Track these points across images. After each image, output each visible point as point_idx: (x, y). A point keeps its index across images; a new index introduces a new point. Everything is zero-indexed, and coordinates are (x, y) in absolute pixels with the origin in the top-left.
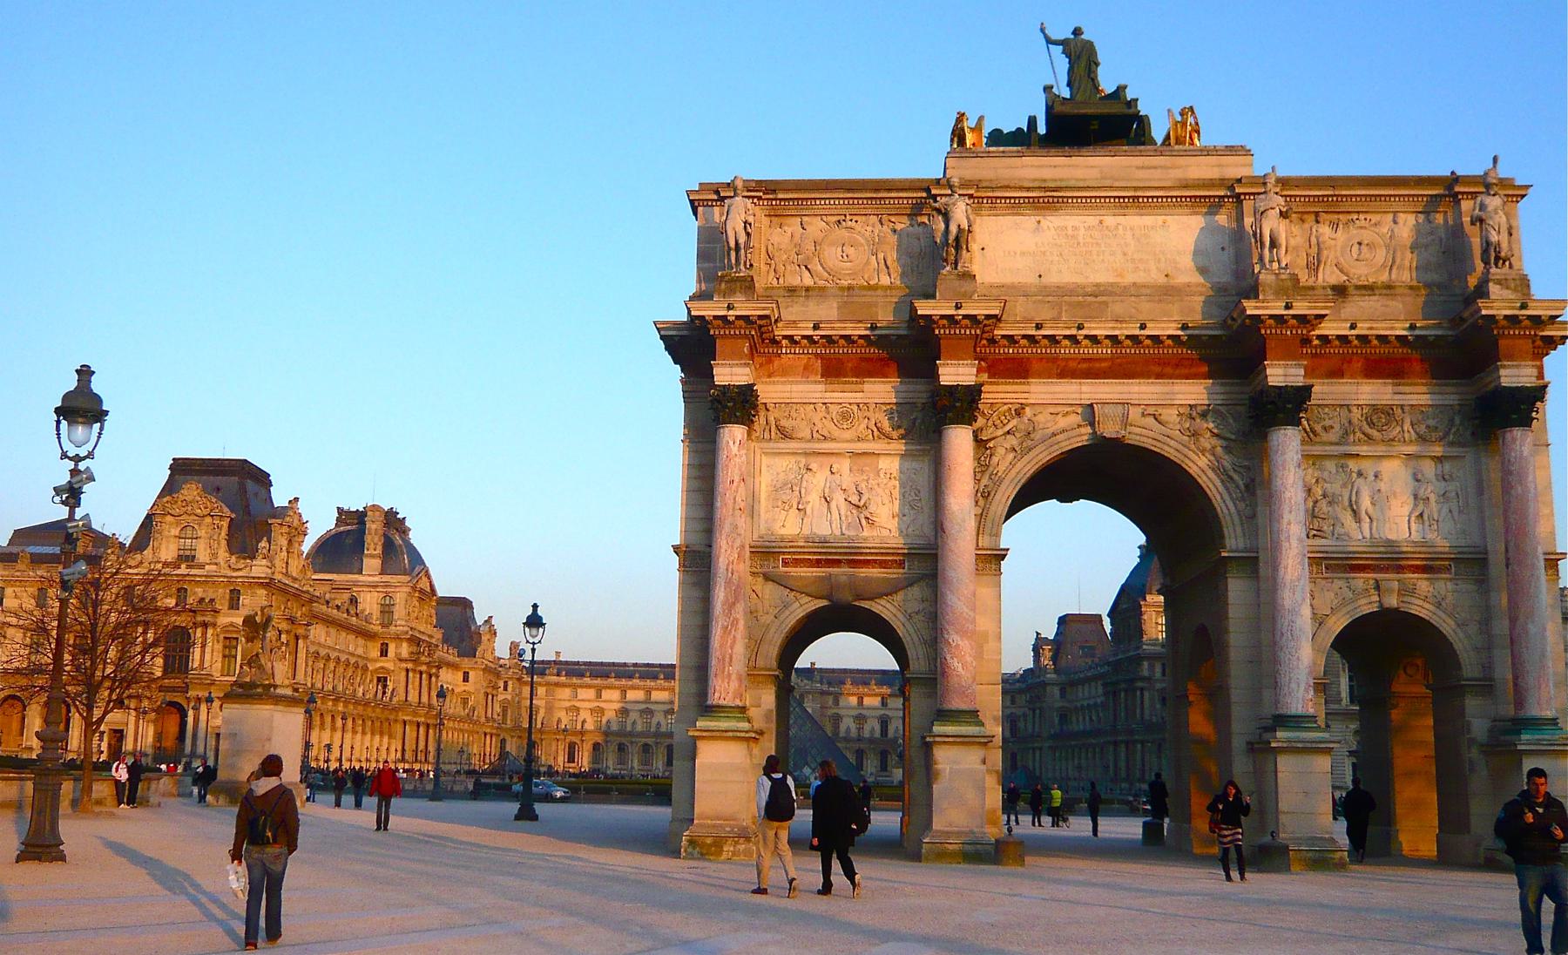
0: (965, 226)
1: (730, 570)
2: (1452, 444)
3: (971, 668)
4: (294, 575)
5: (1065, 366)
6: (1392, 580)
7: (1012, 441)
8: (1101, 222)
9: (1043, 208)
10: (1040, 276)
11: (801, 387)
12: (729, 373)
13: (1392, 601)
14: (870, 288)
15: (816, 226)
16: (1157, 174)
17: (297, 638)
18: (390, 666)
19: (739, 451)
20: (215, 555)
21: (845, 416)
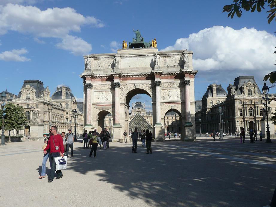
0: (118, 61)
2: (181, 87)
4: (49, 101)
6: (173, 105)
7: (125, 89)
11: (98, 83)
12: (88, 82)
13: (173, 108)
14: (108, 69)
15: (100, 61)
16: (145, 52)
17: (50, 112)
18: (68, 116)
20: (33, 98)
21: (104, 86)
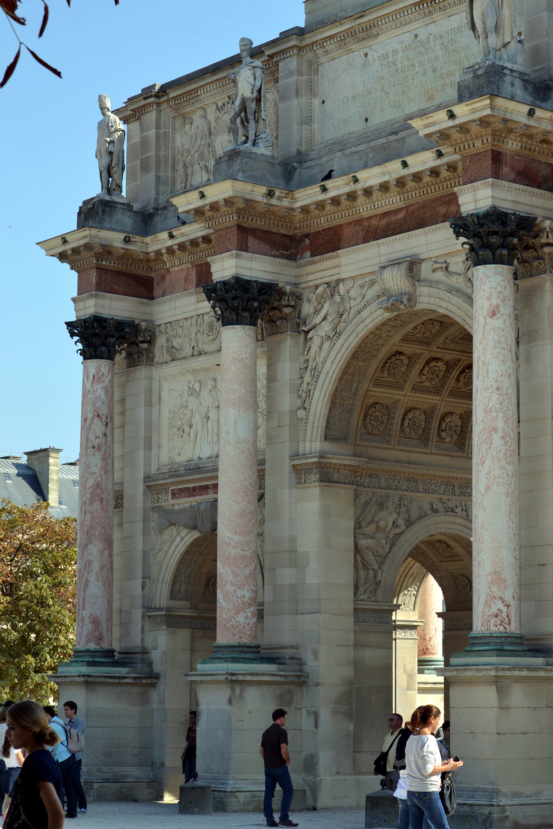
1: (83, 511)
3: (235, 598)
5: (369, 226)
8: (416, 36)
9: (364, 39)
10: (366, 120)
19: (92, 387)
